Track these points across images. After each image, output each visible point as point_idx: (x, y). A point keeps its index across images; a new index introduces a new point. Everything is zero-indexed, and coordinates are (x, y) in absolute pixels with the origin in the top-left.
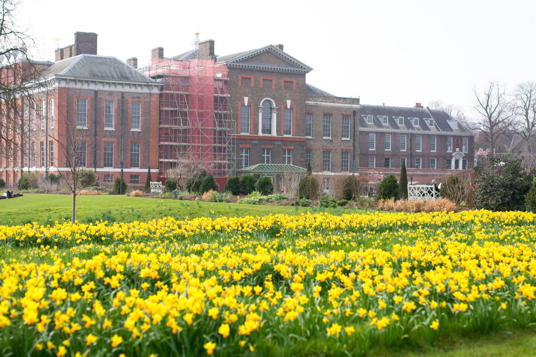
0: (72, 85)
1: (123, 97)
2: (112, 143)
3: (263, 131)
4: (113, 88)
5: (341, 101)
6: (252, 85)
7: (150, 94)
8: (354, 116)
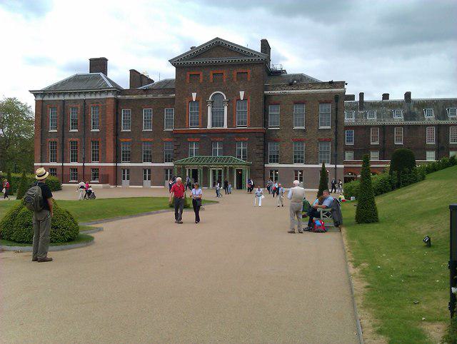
0: (46, 98)
1: (85, 104)
2: (77, 142)
3: (213, 126)
4: (77, 97)
5: (318, 87)
6: (201, 80)
7: (106, 99)
8: (337, 101)
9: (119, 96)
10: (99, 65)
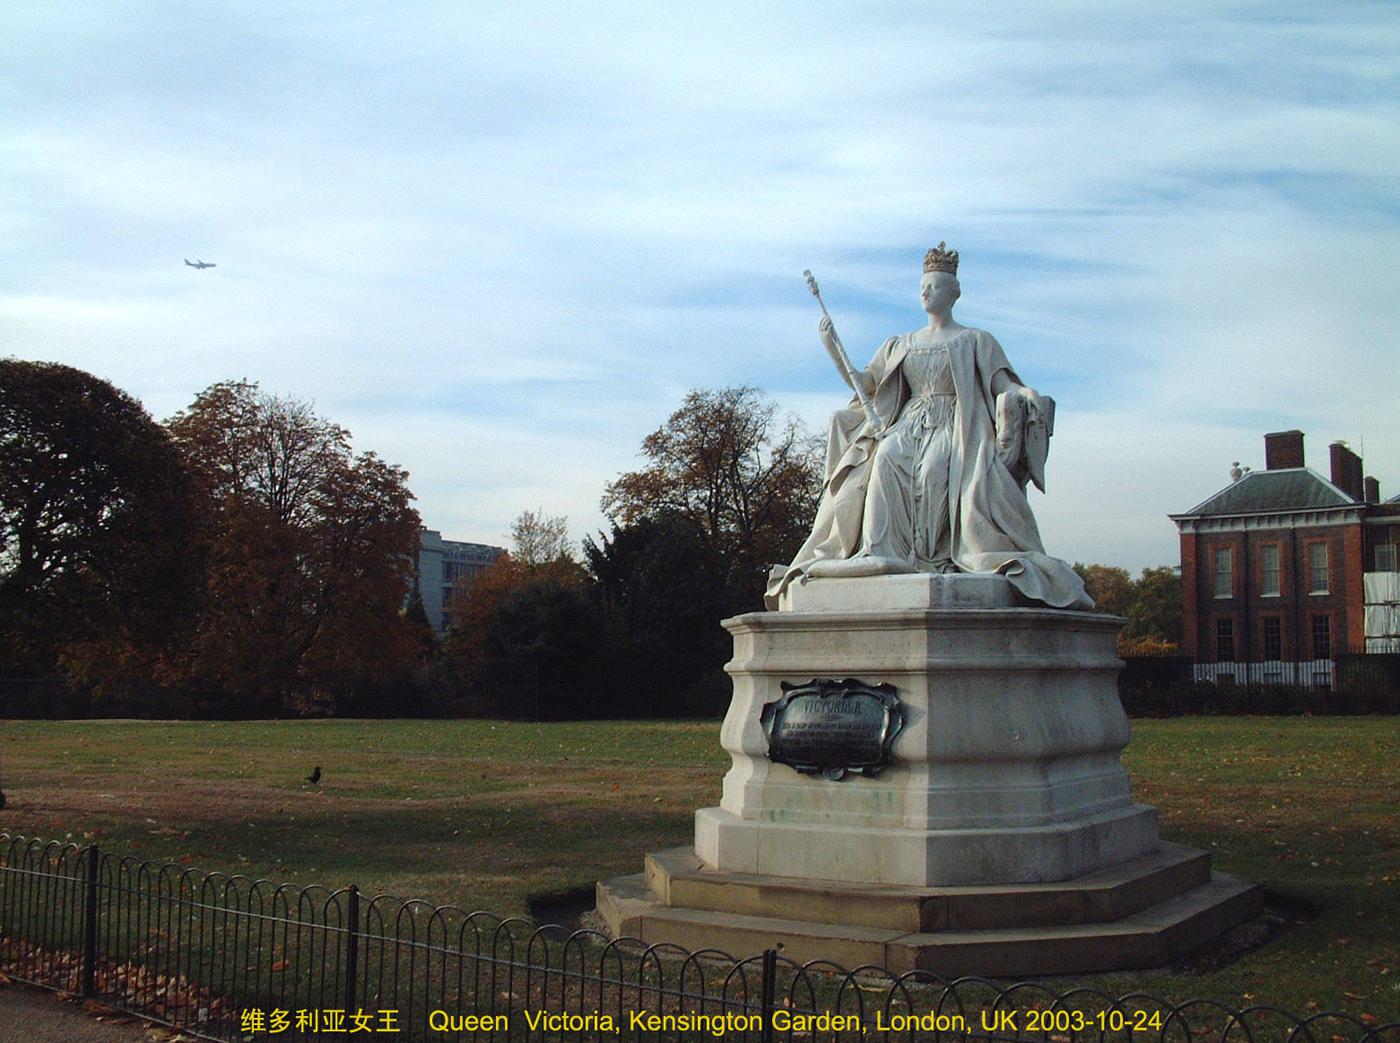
0: (1205, 530)
4: (1275, 526)
9: (1369, 520)
10: (1285, 448)
